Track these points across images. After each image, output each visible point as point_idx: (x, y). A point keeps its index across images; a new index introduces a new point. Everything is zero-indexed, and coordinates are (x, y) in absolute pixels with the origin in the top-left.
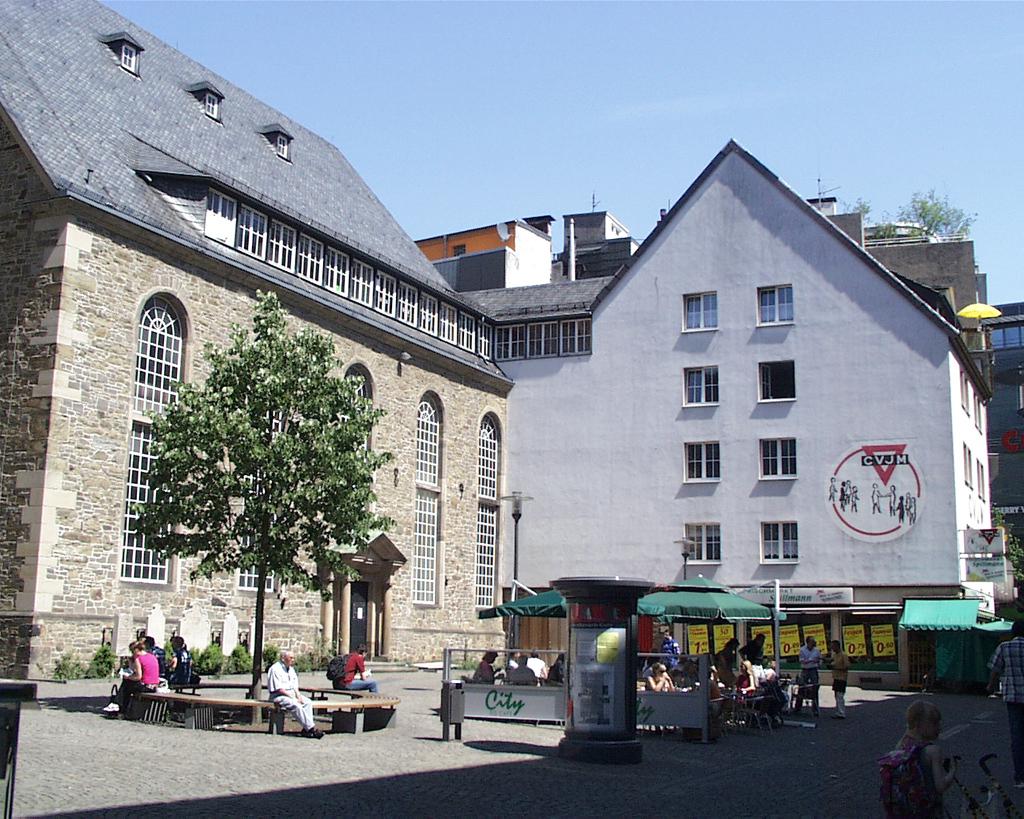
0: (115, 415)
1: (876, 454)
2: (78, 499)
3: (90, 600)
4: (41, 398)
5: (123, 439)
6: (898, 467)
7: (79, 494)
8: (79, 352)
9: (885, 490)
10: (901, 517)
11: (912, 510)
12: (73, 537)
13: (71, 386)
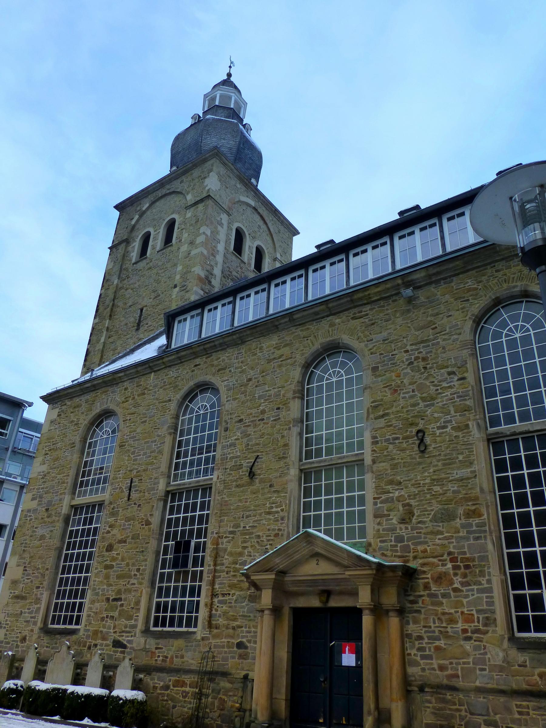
2: (24, 570)
3: (19, 643)
7: (25, 567)
8: (41, 477)
12: (17, 597)
13: (33, 499)
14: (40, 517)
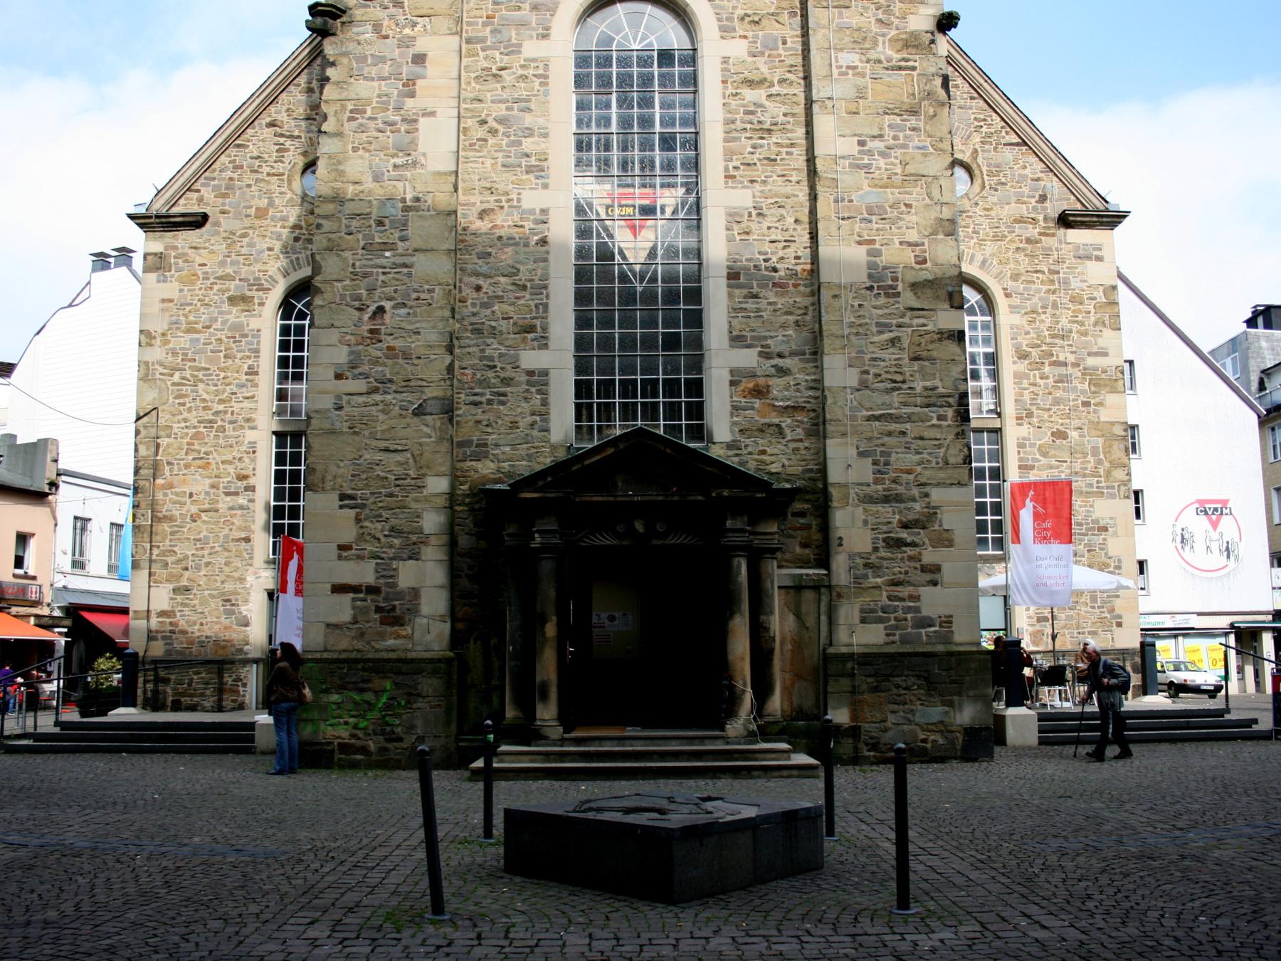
1: (1207, 506)
4: (1112, 423)
6: (1224, 517)
9: (1215, 535)
10: (1228, 557)
11: (1236, 552)
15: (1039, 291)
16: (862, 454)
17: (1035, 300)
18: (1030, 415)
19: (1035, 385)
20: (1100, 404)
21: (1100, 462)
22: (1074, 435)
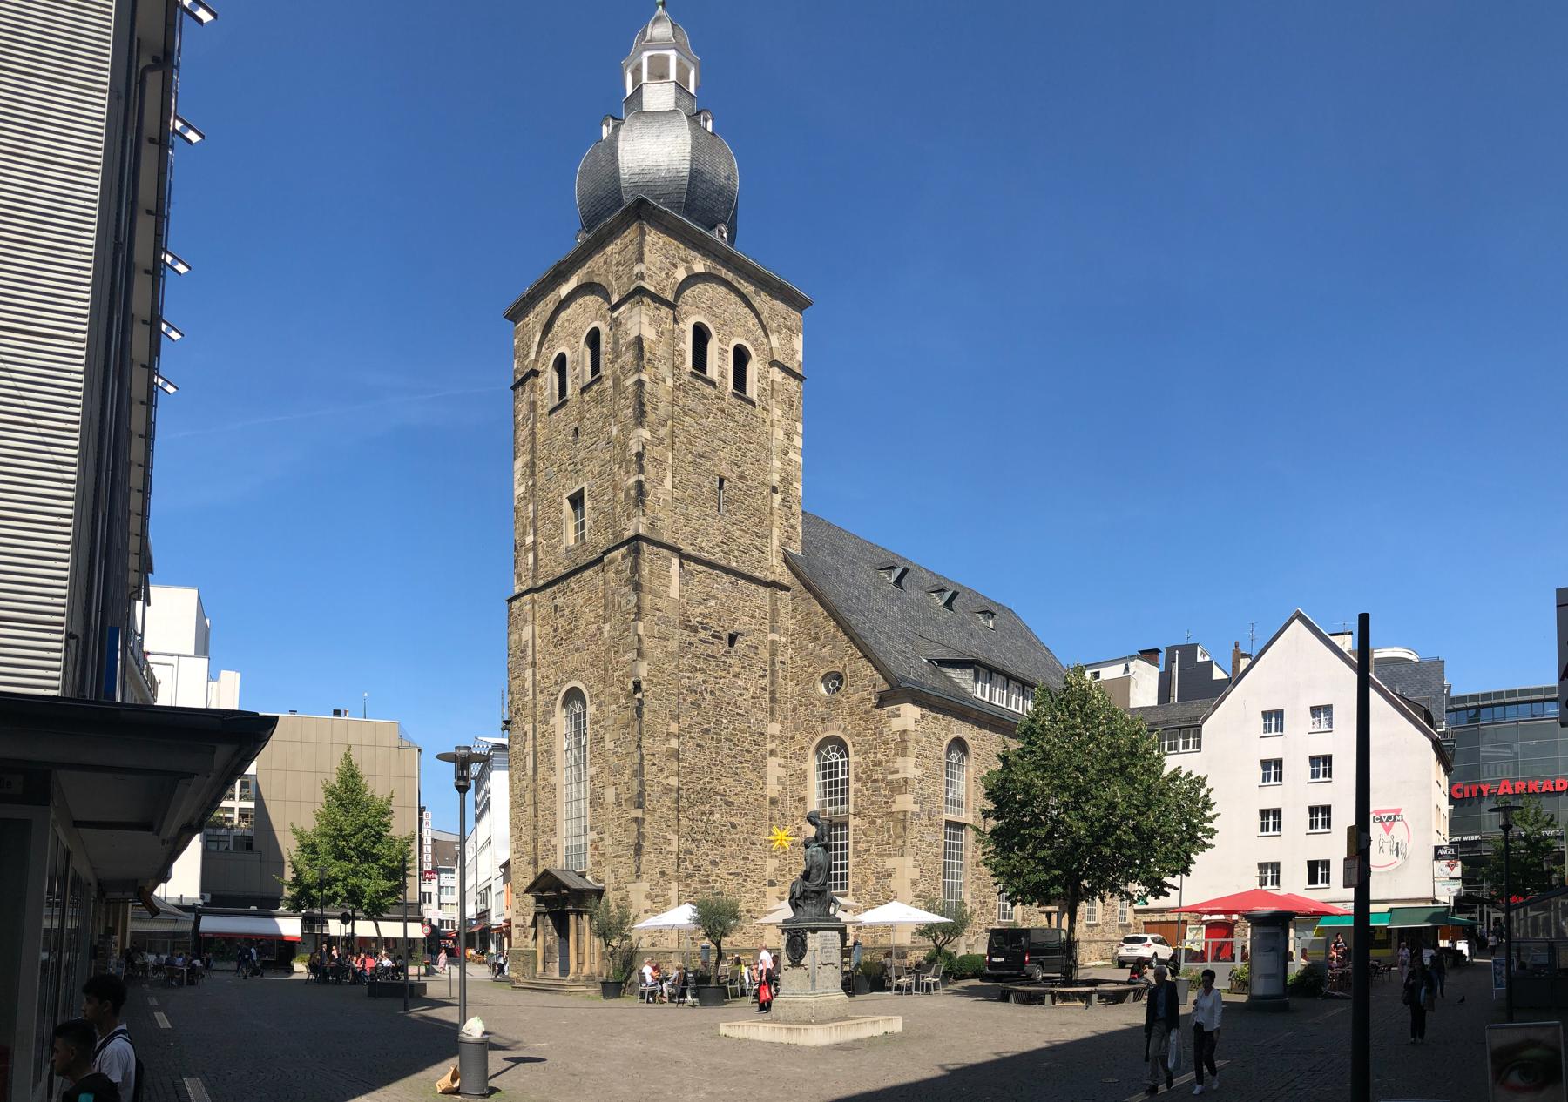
0: (935, 818)
4: (898, 812)
5: (940, 832)
13: (915, 803)
14: (924, 824)
15: (869, 740)
16: (612, 872)
17: (867, 746)
18: (859, 813)
19: (863, 795)
20: (894, 802)
21: (890, 836)
22: (879, 821)
